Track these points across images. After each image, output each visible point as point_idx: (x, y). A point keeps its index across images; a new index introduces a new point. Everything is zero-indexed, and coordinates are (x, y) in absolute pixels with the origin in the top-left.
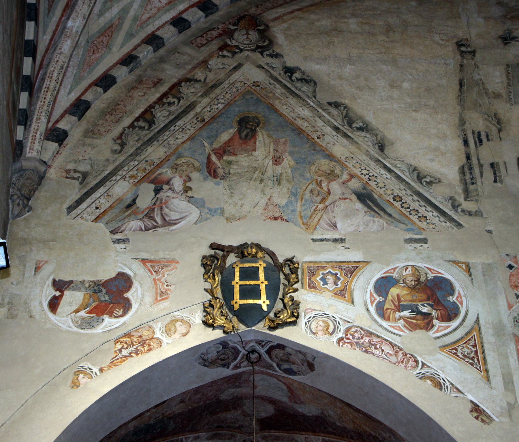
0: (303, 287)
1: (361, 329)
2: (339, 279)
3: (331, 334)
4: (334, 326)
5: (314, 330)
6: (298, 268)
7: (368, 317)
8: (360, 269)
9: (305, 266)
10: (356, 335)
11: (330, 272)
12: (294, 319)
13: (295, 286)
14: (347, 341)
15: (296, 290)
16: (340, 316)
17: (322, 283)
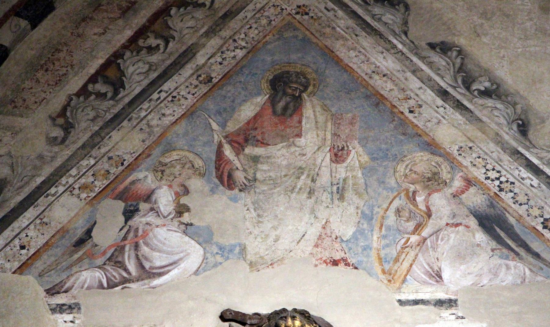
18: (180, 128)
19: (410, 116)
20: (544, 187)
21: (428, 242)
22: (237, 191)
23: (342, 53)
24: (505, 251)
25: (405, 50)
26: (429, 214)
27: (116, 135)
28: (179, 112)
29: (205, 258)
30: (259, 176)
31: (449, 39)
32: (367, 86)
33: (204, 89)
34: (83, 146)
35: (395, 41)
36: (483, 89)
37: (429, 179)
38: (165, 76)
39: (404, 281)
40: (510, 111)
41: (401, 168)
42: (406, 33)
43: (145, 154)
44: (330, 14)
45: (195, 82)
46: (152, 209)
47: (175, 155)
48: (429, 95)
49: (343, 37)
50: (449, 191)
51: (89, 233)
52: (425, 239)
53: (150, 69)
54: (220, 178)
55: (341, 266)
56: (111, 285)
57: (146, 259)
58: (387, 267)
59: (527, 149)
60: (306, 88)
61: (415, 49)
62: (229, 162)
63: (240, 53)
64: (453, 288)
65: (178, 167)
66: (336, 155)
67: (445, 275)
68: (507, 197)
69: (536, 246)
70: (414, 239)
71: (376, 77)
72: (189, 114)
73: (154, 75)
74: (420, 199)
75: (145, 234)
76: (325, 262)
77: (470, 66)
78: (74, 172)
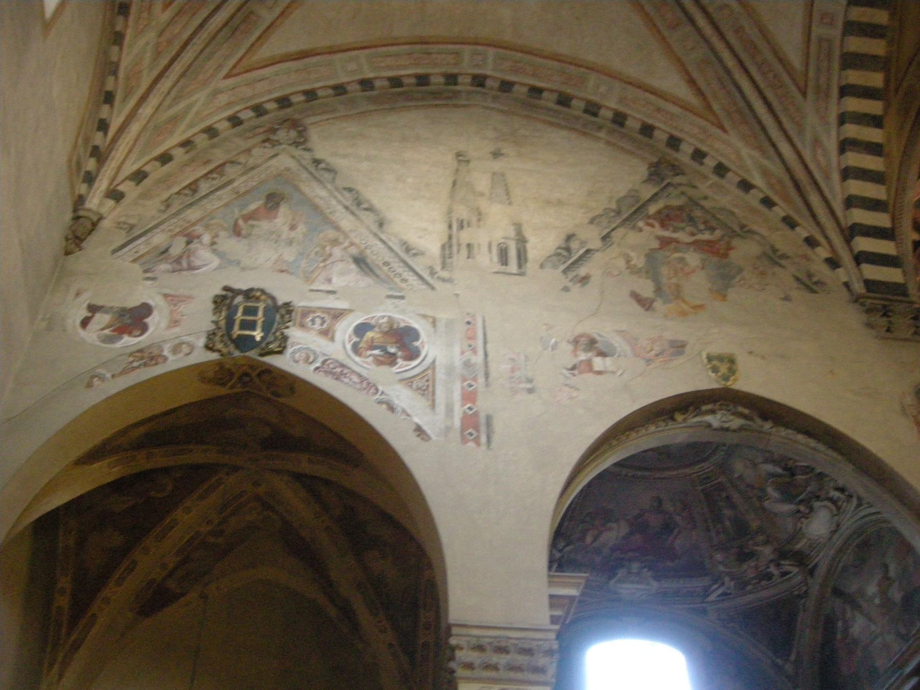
0: (294, 325)
9: (300, 309)
13: (288, 324)
15: (287, 327)
21: (328, 267)
23: (302, 186)
27: (189, 211)
33: (235, 196)
34: (173, 214)
38: (218, 189)
41: (321, 235)
43: (201, 220)
48: (340, 208)
56: (174, 271)
60: (283, 199)
61: (337, 189)
63: (254, 184)
68: (368, 252)
69: (378, 272)
70: (322, 265)
72: (226, 205)
74: (328, 248)
78: (167, 224)
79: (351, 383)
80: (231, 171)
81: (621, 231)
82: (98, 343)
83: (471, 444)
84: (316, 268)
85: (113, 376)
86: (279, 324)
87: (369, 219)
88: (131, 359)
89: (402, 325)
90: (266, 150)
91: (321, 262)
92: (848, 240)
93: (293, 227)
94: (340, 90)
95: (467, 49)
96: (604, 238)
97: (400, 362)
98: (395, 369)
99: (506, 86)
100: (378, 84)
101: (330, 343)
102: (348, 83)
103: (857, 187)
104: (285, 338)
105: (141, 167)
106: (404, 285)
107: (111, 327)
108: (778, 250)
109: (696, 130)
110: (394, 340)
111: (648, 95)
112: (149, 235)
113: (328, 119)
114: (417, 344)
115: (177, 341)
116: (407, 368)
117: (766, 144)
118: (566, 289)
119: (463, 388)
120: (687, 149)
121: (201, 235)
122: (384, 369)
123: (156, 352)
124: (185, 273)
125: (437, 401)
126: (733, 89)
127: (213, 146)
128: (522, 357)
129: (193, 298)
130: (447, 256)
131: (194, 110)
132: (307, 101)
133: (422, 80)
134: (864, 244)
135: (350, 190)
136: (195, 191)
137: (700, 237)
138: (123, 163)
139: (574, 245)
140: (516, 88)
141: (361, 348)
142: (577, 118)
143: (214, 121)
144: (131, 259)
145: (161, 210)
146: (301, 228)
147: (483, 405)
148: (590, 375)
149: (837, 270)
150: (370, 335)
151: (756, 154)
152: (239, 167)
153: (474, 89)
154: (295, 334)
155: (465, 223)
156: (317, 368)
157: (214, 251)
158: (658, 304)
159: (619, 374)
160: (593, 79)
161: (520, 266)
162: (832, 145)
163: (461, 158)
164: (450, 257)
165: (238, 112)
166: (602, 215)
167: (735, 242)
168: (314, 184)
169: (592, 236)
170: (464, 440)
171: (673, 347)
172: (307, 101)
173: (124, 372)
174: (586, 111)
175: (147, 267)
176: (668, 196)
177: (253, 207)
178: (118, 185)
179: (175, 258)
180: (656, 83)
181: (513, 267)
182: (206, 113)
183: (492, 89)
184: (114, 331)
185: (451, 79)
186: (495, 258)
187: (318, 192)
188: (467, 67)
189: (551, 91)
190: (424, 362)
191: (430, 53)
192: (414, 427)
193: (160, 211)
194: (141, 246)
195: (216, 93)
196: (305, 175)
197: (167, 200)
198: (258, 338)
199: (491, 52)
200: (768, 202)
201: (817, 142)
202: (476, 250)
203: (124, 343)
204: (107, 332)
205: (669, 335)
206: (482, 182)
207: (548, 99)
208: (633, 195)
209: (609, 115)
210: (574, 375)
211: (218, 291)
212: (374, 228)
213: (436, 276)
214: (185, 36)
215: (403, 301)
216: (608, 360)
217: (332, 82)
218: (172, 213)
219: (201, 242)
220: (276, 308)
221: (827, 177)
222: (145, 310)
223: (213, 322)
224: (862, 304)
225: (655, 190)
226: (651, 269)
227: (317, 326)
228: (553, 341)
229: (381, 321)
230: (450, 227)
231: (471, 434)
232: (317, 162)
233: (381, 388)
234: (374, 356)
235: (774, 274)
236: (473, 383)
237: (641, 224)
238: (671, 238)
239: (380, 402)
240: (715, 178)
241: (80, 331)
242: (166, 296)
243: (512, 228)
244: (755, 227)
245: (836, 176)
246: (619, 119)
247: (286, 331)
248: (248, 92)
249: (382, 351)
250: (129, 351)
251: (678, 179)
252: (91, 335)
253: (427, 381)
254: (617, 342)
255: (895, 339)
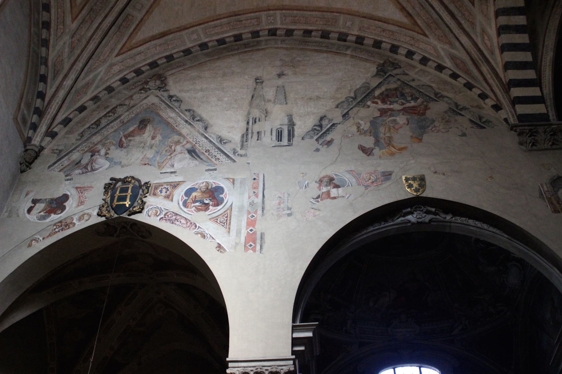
0: (150, 195)
1: (173, 213)
2: (168, 190)
3: (158, 216)
4: (160, 212)
5: (150, 214)
6: (150, 186)
7: (178, 207)
8: (180, 185)
9: (154, 185)
10: (170, 216)
11: (165, 187)
12: (140, 210)
13: (146, 195)
14: (164, 219)
15: (146, 197)
16: (164, 207)
17: (159, 192)
18: (111, 135)
19: (176, 127)
20: (208, 142)
21: (173, 158)
22: (123, 148)
23: (161, 113)
24: (193, 158)
25: (178, 112)
26: (175, 151)
27: (94, 137)
28: (113, 130)
29: (110, 165)
30: (130, 144)
31: (191, 108)
32: (165, 120)
33: (121, 124)
34: (85, 140)
35: (176, 110)
36: (197, 119)
37: (177, 142)
38: (112, 122)
39: (163, 167)
40: (204, 124)
41: (170, 140)
42: (180, 108)
43: (101, 141)
44: (161, 104)
45: (119, 123)
46: (99, 154)
47: (108, 141)
48: (183, 122)
49: (162, 110)
50: (181, 145)
51: (80, 161)
52: (172, 157)
53: (108, 121)
54: (119, 146)
55: (147, 165)
56: (83, 173)
57: (94, 166)
58: (159, 164)
59: (206, 133)
60: (149, 122)
61: (182, 112)
62: (123, 141)
63: (133, 115)
64: (176, 168)
65: (109, 144)
66: (153, 138)
67: (175, 166)
68: (197, 145)
69: (202, 157)
70: (169, 157)
71: (169, 118)
72: (115, 131)
73: (109, 122)
74: (173, 147)
75: (95, 160)
76: (143, 164)
77: (195, 114)
78: (81, 147)
79: (181, 225)
80: (120, 110)
81: (356, 109)
82: (37, 221)
83: (251, 251)
84: (166, 159)
85: (43, 239)
86: (141, 195)
87: (199, 126)
88: (55, 227)
89: (214, 186)
90: (142, 95)
91: (169, 156)
92: (507, 91)
93: (153, 138)
94: (187, 52)
95: (263, 15)
96: (344, 116)
97: (211, 207)
98: (208, 213)
99: (289, 33)
100: (210, 44)
101: (170, 203)
102: (192, 47)
103: (510, 56)
104: (143, 203)
105: (67, 116)
106: (217, 162)
107: (45, 210)
108: (460, 105)
109: (408, 39)
110: (208, 195)
111: (377, 22)
112: (71, 154)
113: (180, 71)
114: (221, 196)
115: (81, 213)
116: (214, 211)
117: (454, 40)
118: (317, 150)
119: (248, 218)
120: (403, 51)
121: (100, 150)
122: (202, 213)
123: (69, 221)
124: (88, 173)
125: (232, 228)
126: (430, 9)
127: (111, 97)
128: (286, 195)
129: (93, 188)
130: (245, 141)
131: (99, 77)
132: (168, 62)
133: (238, 38)
134: (516, 92)
135: (189, 110)
136: (98, 125)
137: (408, 105)
138: (56, 115)
139: (324, 123)
140: (295, 32)
141: (188, 203)
142: (333, 44)
143: (111, 83)
144: (59, 170)
145: (78, 139)
146: (159, 137)
147: (259, 228)
148: (329, 200)
149: (499, 112)
150: (194, 194)
151: (447, 47)
152: (125, 107)
153: (270, 37)
154: (150, 200)
155: (257, 120)
156: (162, 218)
157: (107, 159)
158: (377, 151)
159: (347, 197)
160: (342, 18)
161: (289, 140)
162: (492, 31)
163: (258, 81)
164: (246, 142)
165: (126, 75)
166: (344, 102)
167: (431, 105)
168: (168, 110)
169: (337, 116)
170: (246, 249)
171: (383, 176)
172: (168, 62)
173: (50, 235)
174: (339, 39)
175: (68, 172)
176: (388, 83)
177: (131, 129)
178: (54, 128)
179: (85, 165)
180: (380, 14)
181: (285, 141)
182: (106, 79)
183: (281, 36)
184: (45, 213)
185: (255, 34)
186: (274, 138)
187: (169, 115)
188: (265, 25)
189: (317, 30)
190: (225, 207)
191: (242, 21)
192: (216, 245)
193: (77, 140)
194: (65, 162)
195: (112, 66)
196: (163, 105)
197: (82, 133)
198: (127, 206)
199: (278, 12)
200: (454, 76)
201: (483, 31)
202: (263, 135)
203: (51, 219)
204: (42, 213)
205: (380, 169)
206: (270, 93)
207: (316, 37)
208: (366, 86)
209: (354, 39)
210: (318, 202)
211: (108, 181)
212: (202, 131)
213: (237, 154)
214: (90, 34)
215: (215, 172)
216: (340, 190)
217: (183, 48)
218: (84, 140)
219: (99, 155)
220: (141, 186)
221: (492, 53)
222: (65, 197)
223: (103, 199)
224: (515, 131)
225: (381, 80)
226: (374, 131)
227: (164, 194)
228: (306, 182)
229: (201, 185)
230: (248, 123)
231: (251, 245)
232: (171, 97)
233: (198, 225)
234: (195, 206)
235: (456, 121)
236: (254, 215)
237: (369, 103)
238: (388, 109)
239: (197, 233)
240: (420, 67)
241: (27, 215)
242: (77, 188)
243: (287, 118)
244: (445, 94)
245: (497, 52)
246: (360, 40)
247: (144, 199)
248: (131, 62)
249: (201, 203)
250: (54, 223)
251: (395, 72)
252: (33, 217)
253: (227, 217)
254: (348, 177)
255: (539, 150)
